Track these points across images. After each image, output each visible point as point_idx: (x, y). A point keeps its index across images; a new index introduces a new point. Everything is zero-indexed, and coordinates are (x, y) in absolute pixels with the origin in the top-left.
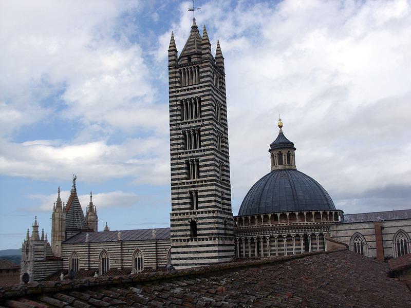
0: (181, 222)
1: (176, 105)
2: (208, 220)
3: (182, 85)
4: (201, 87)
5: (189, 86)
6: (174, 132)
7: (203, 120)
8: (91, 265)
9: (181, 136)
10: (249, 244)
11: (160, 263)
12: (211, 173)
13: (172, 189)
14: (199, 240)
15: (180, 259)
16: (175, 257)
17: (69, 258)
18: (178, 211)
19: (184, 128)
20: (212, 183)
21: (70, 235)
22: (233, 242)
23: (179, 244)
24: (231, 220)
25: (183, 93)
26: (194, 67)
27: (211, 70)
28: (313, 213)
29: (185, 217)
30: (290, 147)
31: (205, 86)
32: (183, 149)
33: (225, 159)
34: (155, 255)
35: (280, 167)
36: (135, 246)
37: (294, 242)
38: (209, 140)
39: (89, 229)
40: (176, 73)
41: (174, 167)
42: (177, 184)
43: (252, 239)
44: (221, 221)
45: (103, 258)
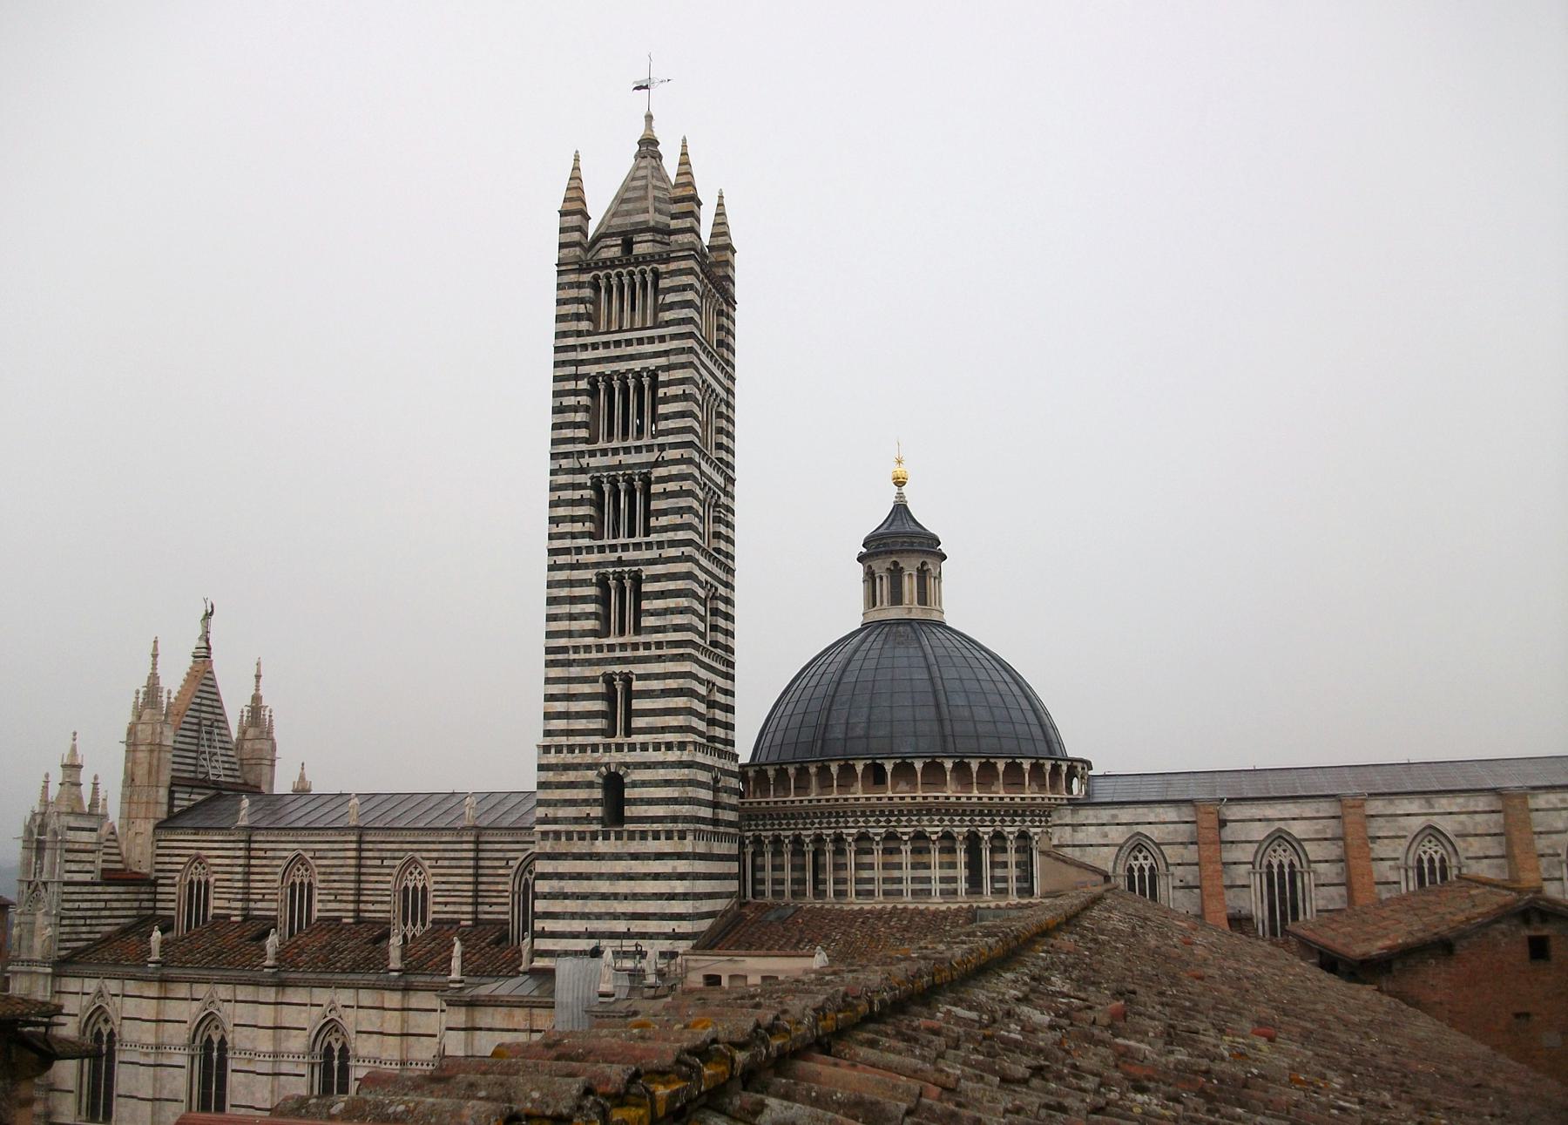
0: (571, 776)
1: (576, 393)
2: (661, 774)
3: (597, 325)
4: (662, 339)
5: (620, 330)
6: (563, 479)
8: (252, 905)
9: (588, 493)
10: (787, 857)
11: (487, 908)
12: (679, 620)
13: (549, 664)
14: (632, 836)
15: (566, 896)
16: (547, 890)
17: (177, 876)
18: (563, 740)
19: (597, 469)
20: (681, 651)
21: (183, 800)
22: (733, 849)
23: (563, 846)
24: (732, 774)
25: (601, 353)
26: (643, 273)
27: (697, 285)
28: (1001, 766)
29: (589, 757)
30: (927, 547)
31: (674, 337)
32: (591, 535)
33: (723, 576)
34: (470, 879)
35: (895, 613)
36: (406, 846)
37: (935, 857)
38: (680, 511)
39: (246, 784)
40: (580, 285)
41: (557, 592)
42: (564, 650)
43: (797, 841)
44: (703, 776)
45: (293, 884)
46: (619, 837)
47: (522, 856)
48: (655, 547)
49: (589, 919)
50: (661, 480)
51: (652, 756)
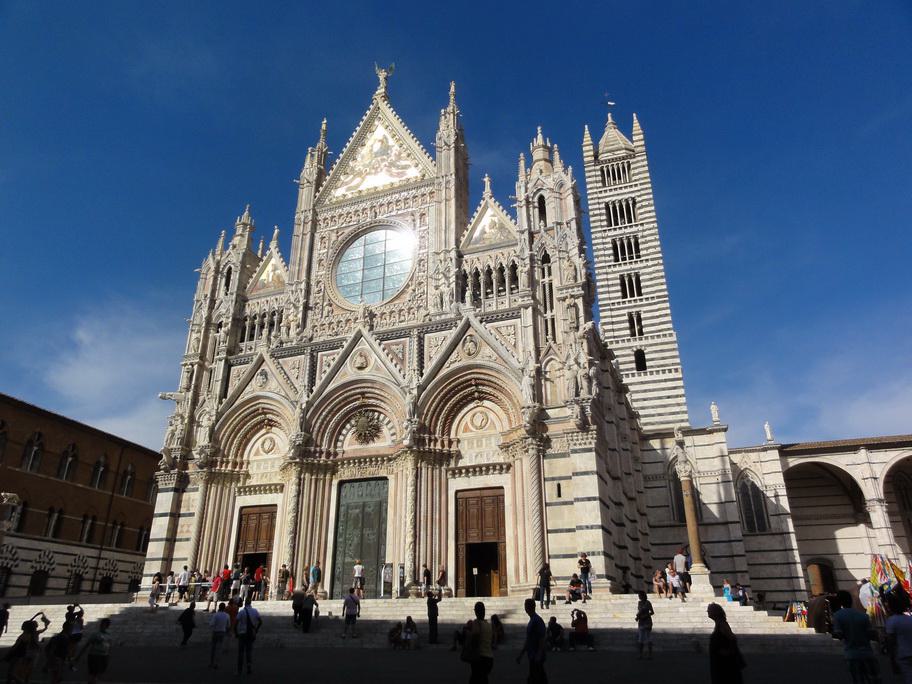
4: (636, 185)
14: (651, 373)
29: (627, 344)
42: (608, 305)
46: (646, 374)
50: (643, 237)
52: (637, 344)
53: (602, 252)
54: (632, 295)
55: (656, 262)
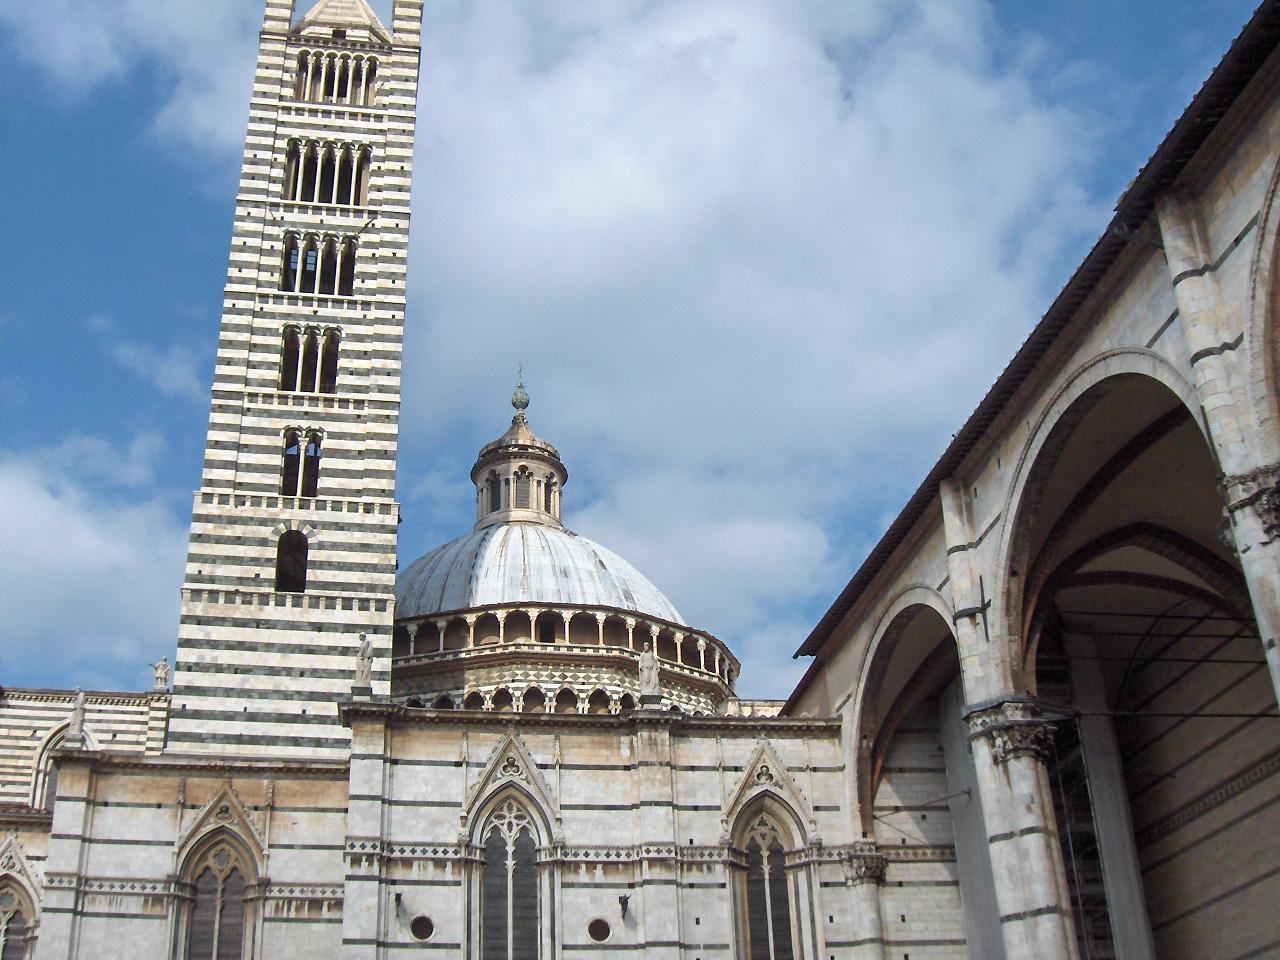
0: (238, 530)
1: (273, 149)
2: (357, 537)
4: (379, 118)
7: (373, 214)
14: (315, 602)
15: (219, 669)
18: (229, 491)
19: (294, 224)
23: (220, 609)
26: (359, 59)
29: (263, 511)
38: (393, 276)
40: (286, 56)
42: (239, 395)
46: (297, 603)
47: (56, 725)
48: (359, 307)
49: (250, 697)
50: (368, 245)
51: (345, 516)
52: (295, 515)
53: (253, 258)
54: (308, 386)
55: (386, 314)
